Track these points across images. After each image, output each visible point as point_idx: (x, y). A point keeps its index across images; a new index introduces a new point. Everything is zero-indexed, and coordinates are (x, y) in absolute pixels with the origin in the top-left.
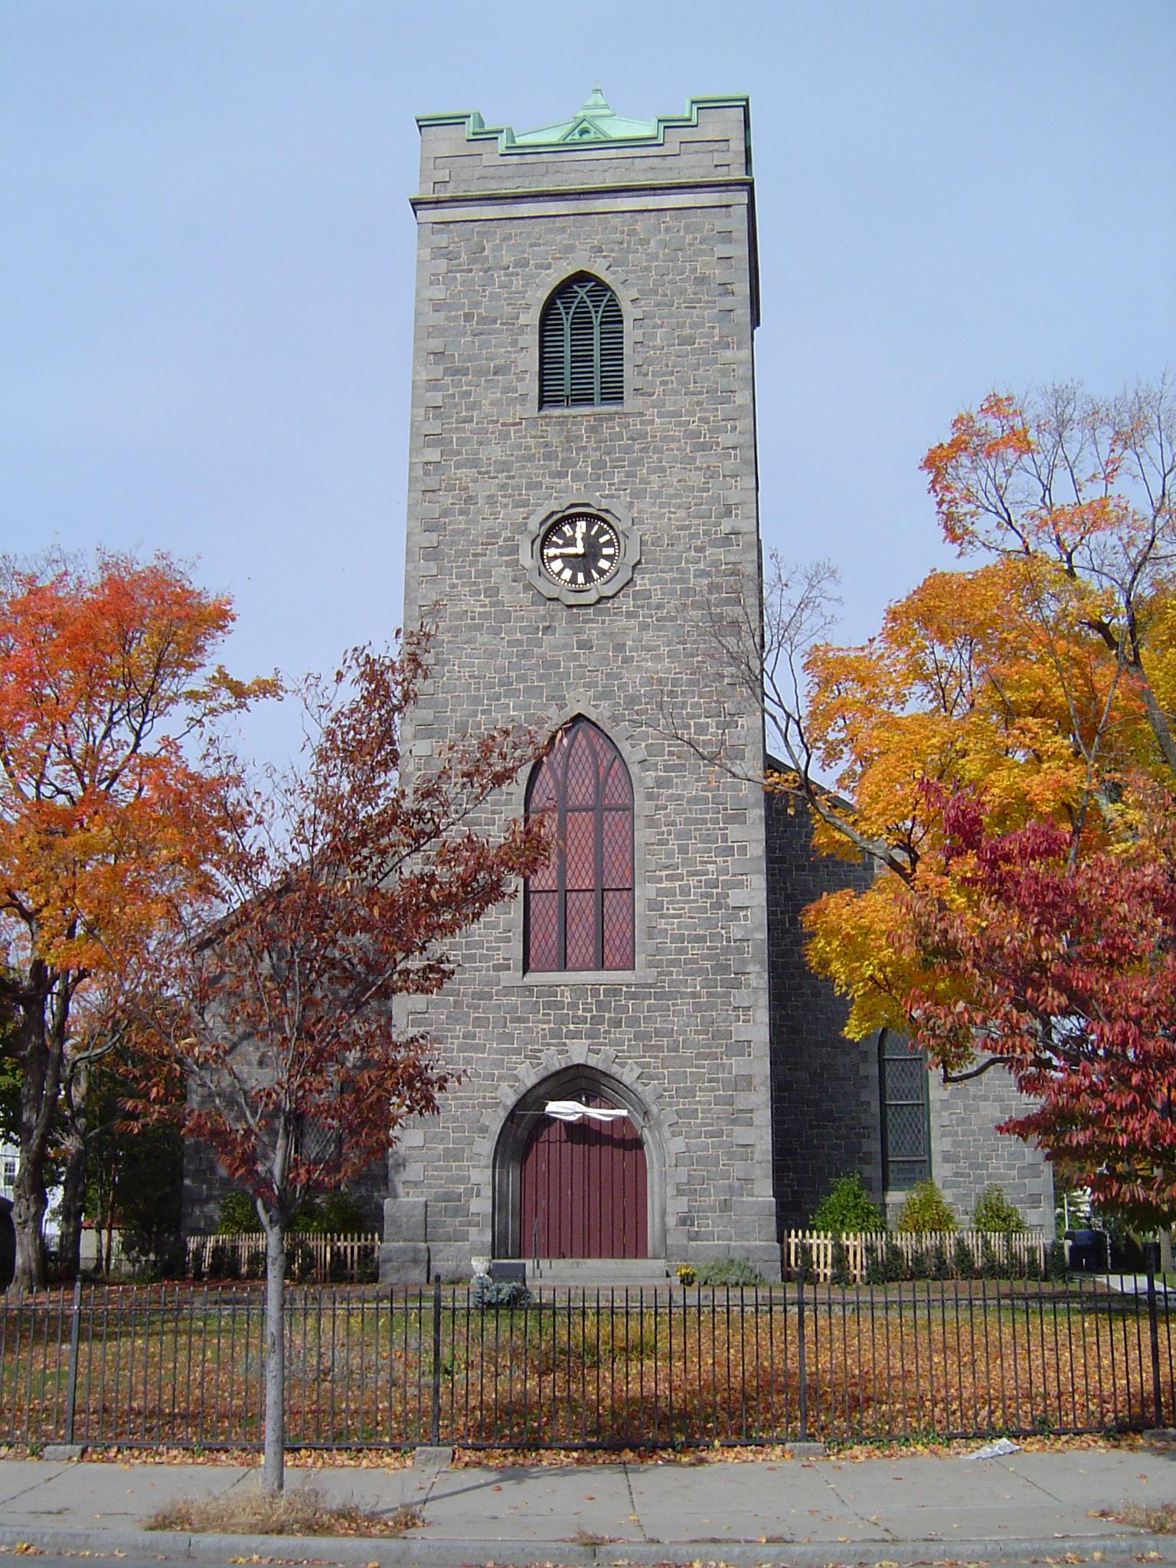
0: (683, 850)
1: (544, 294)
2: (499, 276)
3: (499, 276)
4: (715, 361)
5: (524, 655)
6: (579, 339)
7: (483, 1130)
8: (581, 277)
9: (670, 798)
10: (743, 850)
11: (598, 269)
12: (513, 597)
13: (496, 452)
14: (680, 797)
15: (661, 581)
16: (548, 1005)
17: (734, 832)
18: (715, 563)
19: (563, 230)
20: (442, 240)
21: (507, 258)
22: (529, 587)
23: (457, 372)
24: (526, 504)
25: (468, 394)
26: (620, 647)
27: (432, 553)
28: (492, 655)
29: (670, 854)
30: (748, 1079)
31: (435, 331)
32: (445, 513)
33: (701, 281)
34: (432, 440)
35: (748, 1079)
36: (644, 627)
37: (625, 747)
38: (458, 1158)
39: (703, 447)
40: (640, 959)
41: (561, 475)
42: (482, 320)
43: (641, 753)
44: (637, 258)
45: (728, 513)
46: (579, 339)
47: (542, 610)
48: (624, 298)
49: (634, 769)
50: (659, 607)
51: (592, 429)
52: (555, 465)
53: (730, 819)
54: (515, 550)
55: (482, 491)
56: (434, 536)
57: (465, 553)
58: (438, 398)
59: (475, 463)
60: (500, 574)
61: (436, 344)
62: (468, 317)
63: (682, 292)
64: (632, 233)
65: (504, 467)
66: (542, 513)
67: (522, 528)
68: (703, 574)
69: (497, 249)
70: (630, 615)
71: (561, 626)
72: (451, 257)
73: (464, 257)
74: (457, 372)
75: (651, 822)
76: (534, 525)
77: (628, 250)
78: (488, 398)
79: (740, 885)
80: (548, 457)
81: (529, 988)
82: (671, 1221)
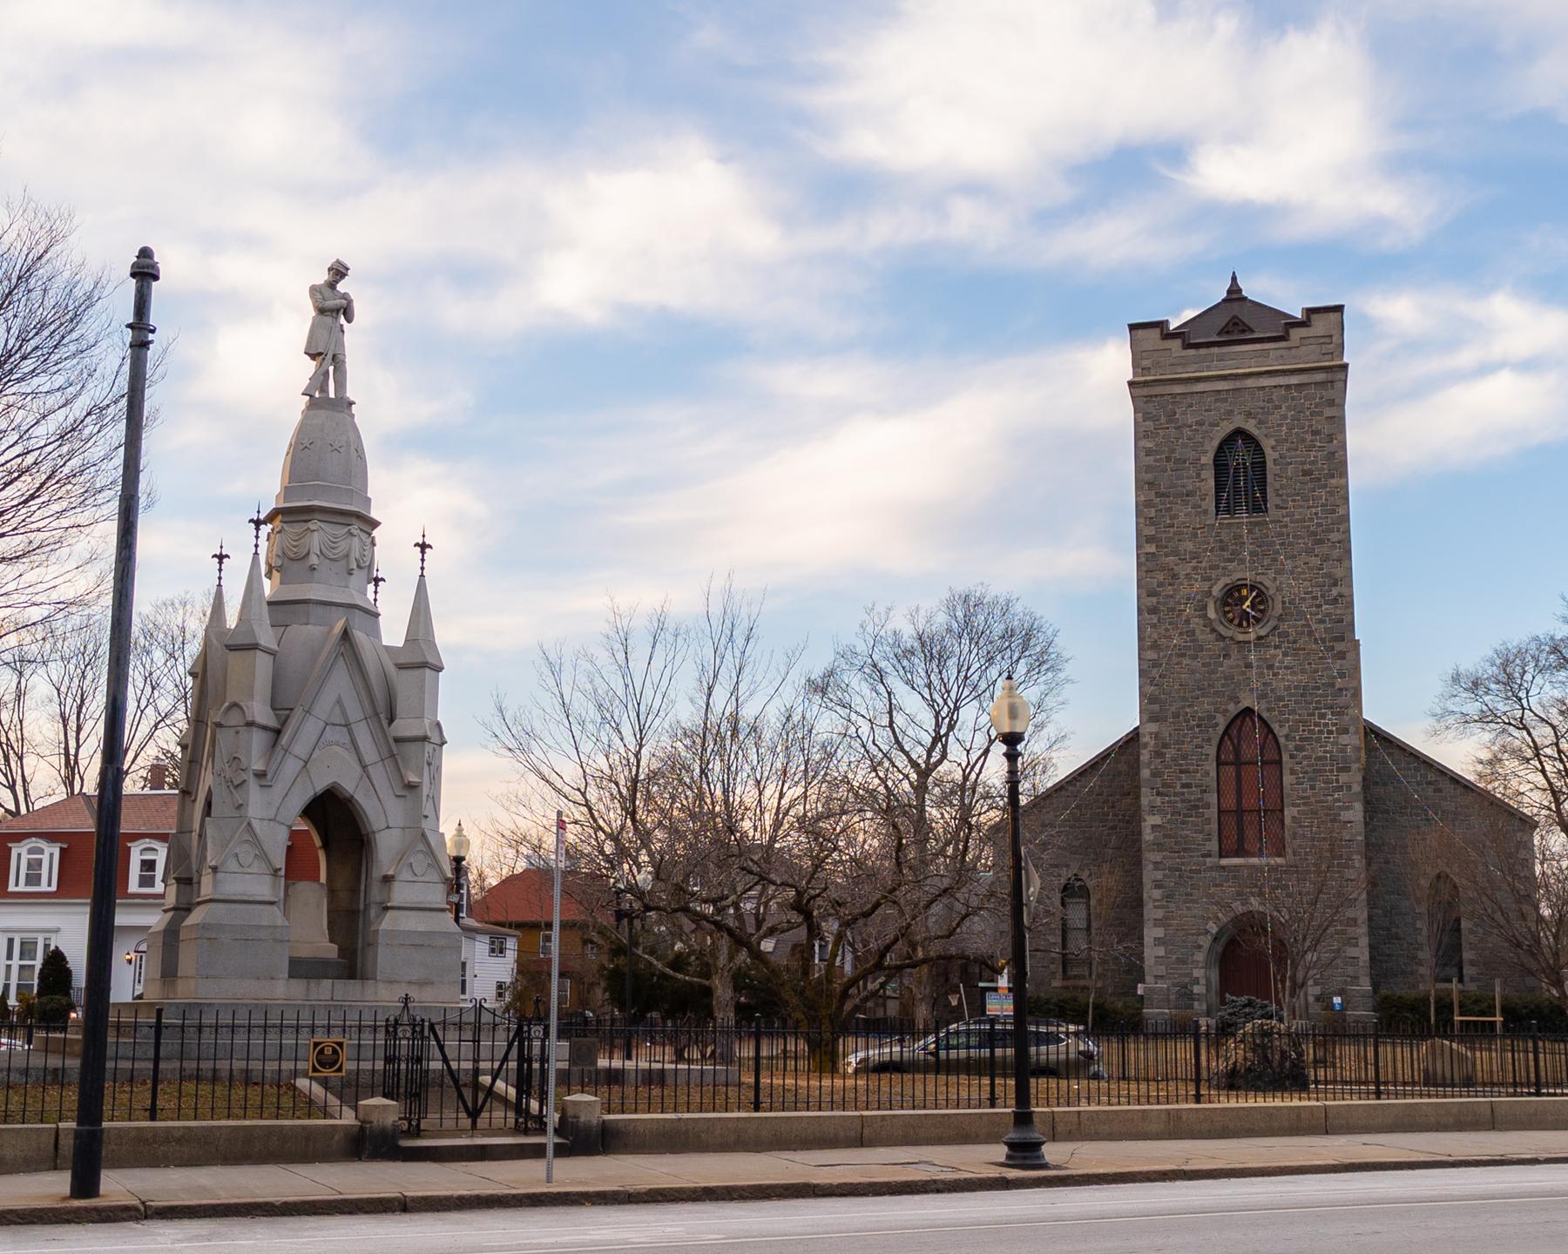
0: (1313, 788)
1: (1216, 443)
2: (1186, 431)
3: (1186, 431)
4: (1325, 486)
5: (1213, 672)
6: (1240, 474)
7: (1200, 947)
8: (1239, 433)
9: (1305, 757)
10: (1349, 788)
11: (1250, 426)
12: (1204, 636)
13: (1189, 546)
14: (1309, 757)
15: (1296, 626)
16: (1235, 877)
17: (1343, 778)
18: (1328, 615)
19: (1225, 400)
20: (1151, 408)
21: (1191, 420)
22: (1213, 630)
23: (1163, 495)
24: (1209, 579)
25: (1170, 509)
26: (1270, 667)
27: (1153, 610)
28: (1193, 672)
29: (1304, 791)
30: (1355, 920)
31: (1148, 469)
32: (1160, 585)
33: (1315, 433)
34: (1150, 539)
35: (1355, 920)
36: (1285, 654)
37: (1276, 727)
38: (1184, 962)
39: (1320, 542)
40: (1289, 850)
41: (1230, 561)
42: (1177, 461)
43: (1285, 731)
44: (1274, 418)
45: (1335, 585)
46: (1240, 474)
47: (1222, 644)
48: (1267, 444)
49: (1282, 740)
50: (1295, 642)
51: (1250, 532)
52: (1226, 554)
53: (1340, 770)
54: (1205, 608)
55: (1183, 570)
56: (1154, 600)
57: (1173, 610)
58: (1152, 513)
59: (1175, 553)
60: (1196, 622)
61: (1149, 477)
62: (1168, 459)
63: (1304, 440)
64: (1270, 401)
65: (1195, 556)
66: (1221, 584)
67: (1209, 593)
68: (1321, 621)
69: (1184, 413)
70: (1276, 647)
71: (1234, 654)
72: (1155, 419)
73: (1163, 420)
74: (1163, 495)
75: (1293, 772)
76: (1216, 591)
77: (1268, 413)
78: (1183, 513)
79: (1348, 808)
80: (1222, 549)
81: (1223, 867)
82: (1311, 999)
